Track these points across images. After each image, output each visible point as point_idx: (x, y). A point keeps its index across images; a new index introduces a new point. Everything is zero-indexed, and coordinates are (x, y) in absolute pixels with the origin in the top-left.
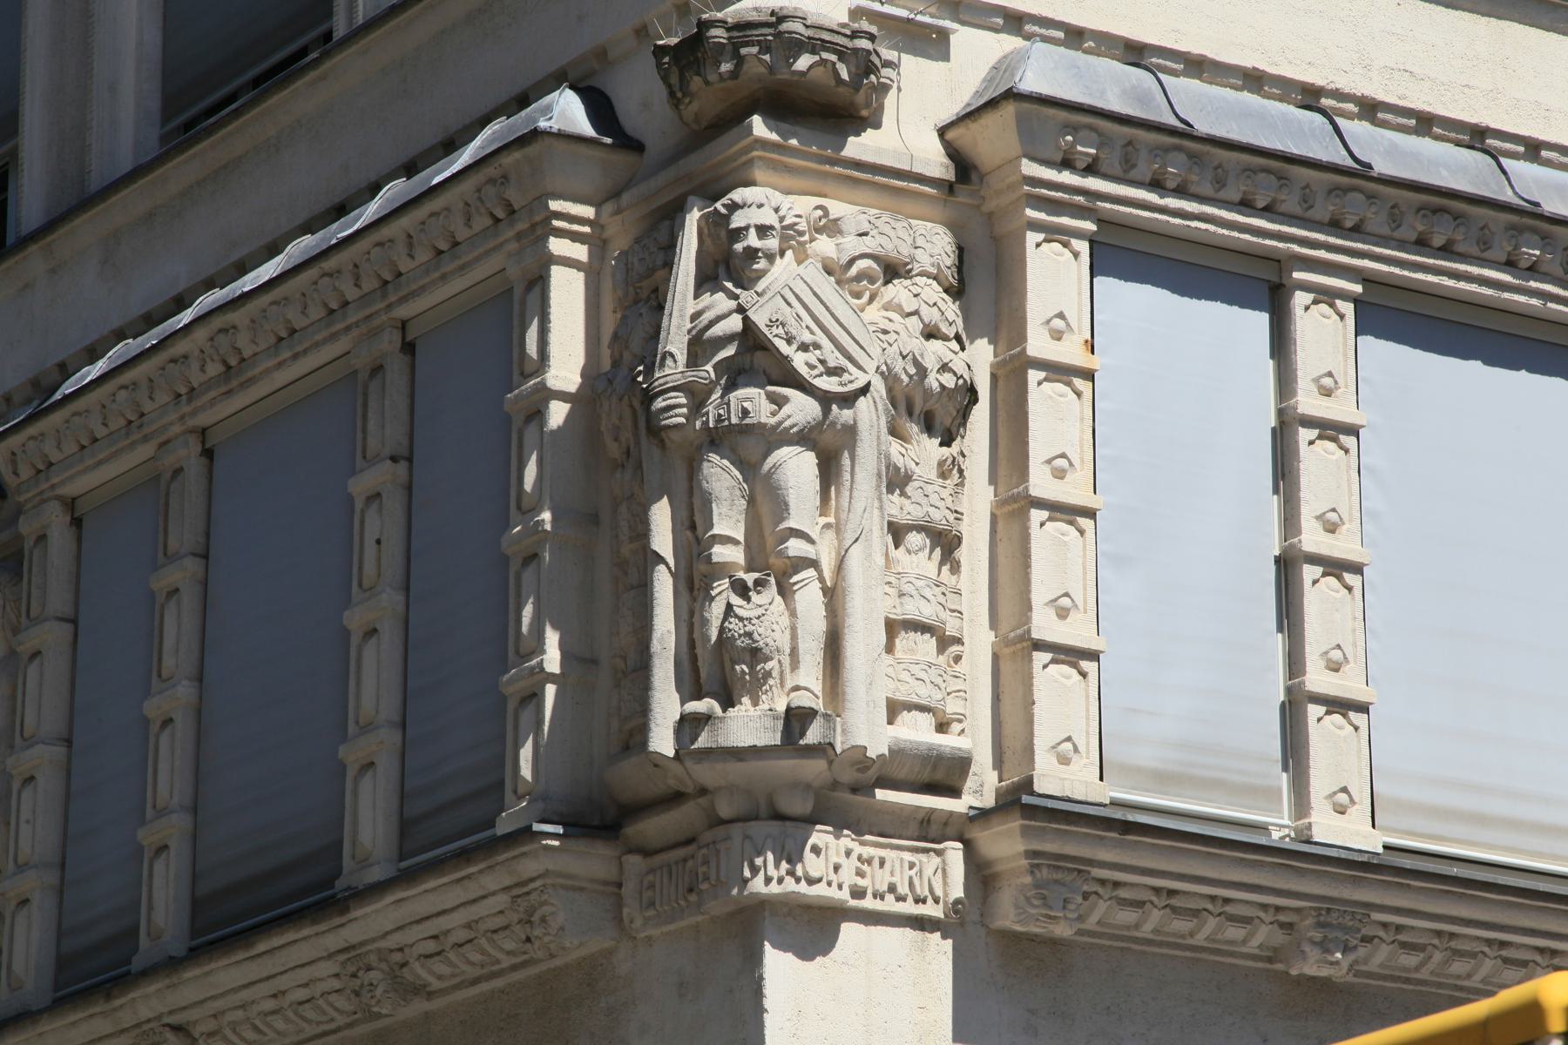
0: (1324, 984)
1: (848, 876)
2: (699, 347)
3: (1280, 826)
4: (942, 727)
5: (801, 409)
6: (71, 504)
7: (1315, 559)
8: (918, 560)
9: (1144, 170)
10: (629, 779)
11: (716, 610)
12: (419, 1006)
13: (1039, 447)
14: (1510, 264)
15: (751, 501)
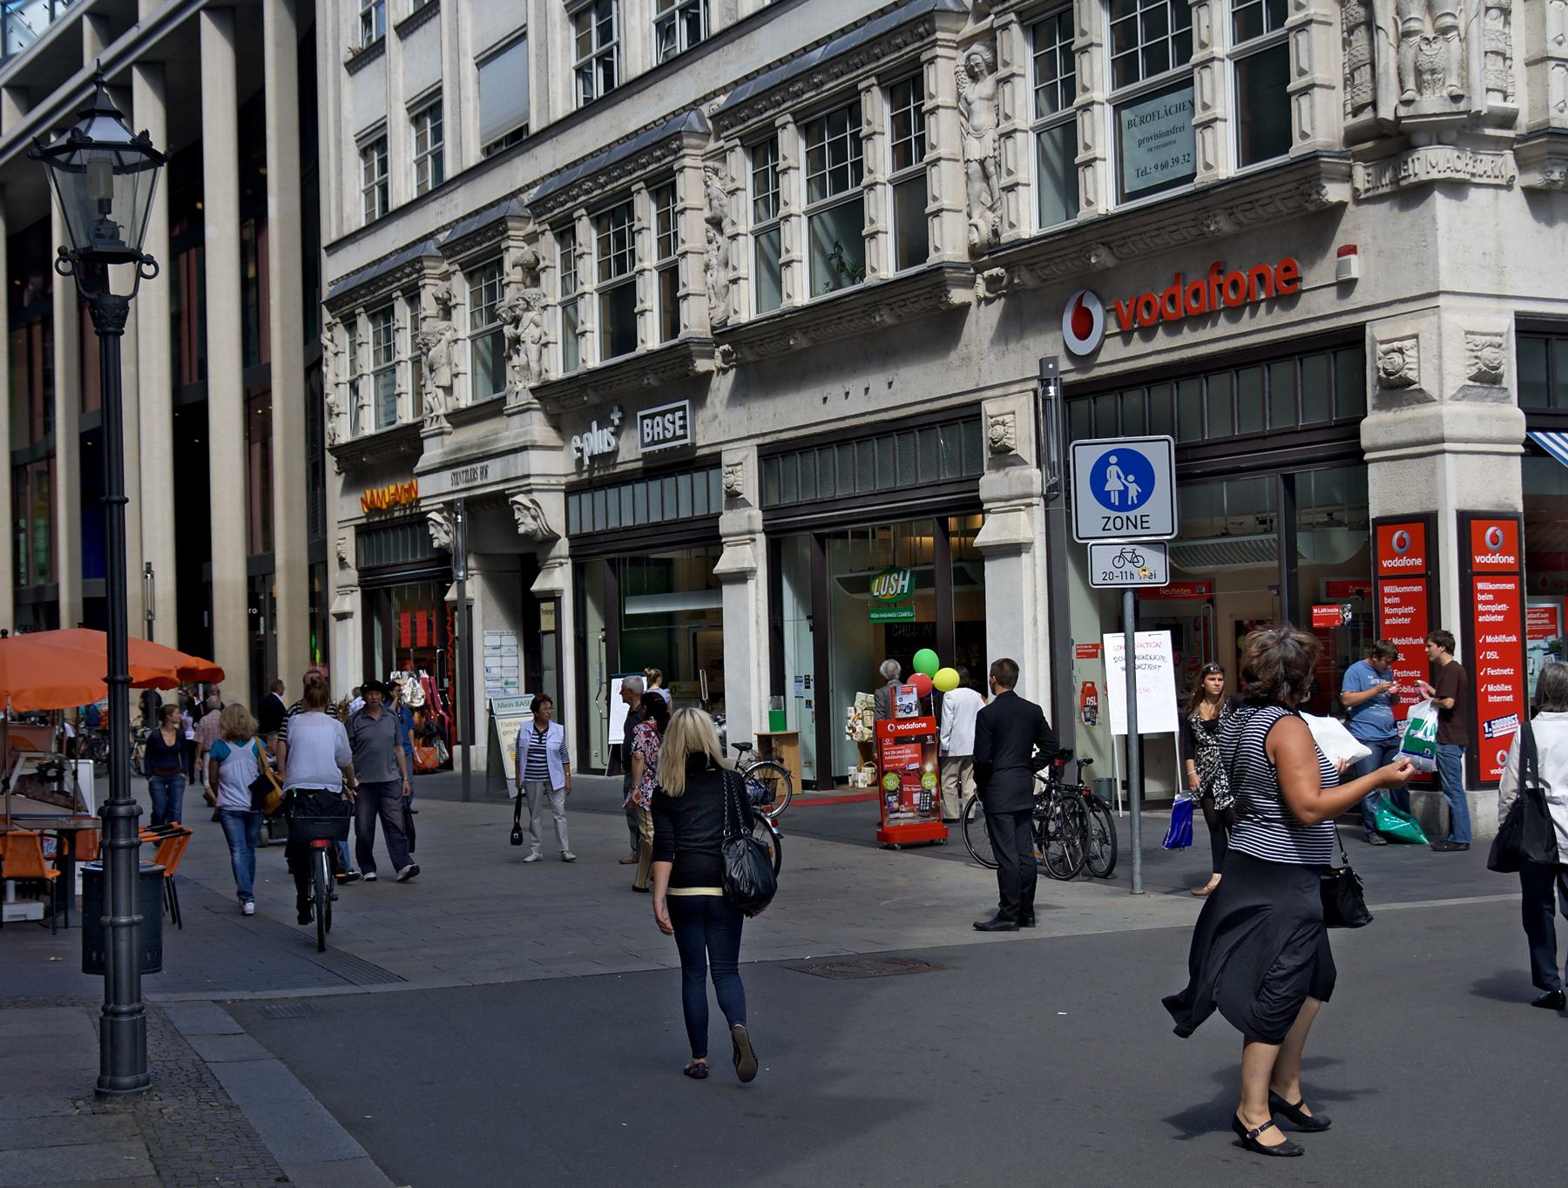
4: (1505, 99)
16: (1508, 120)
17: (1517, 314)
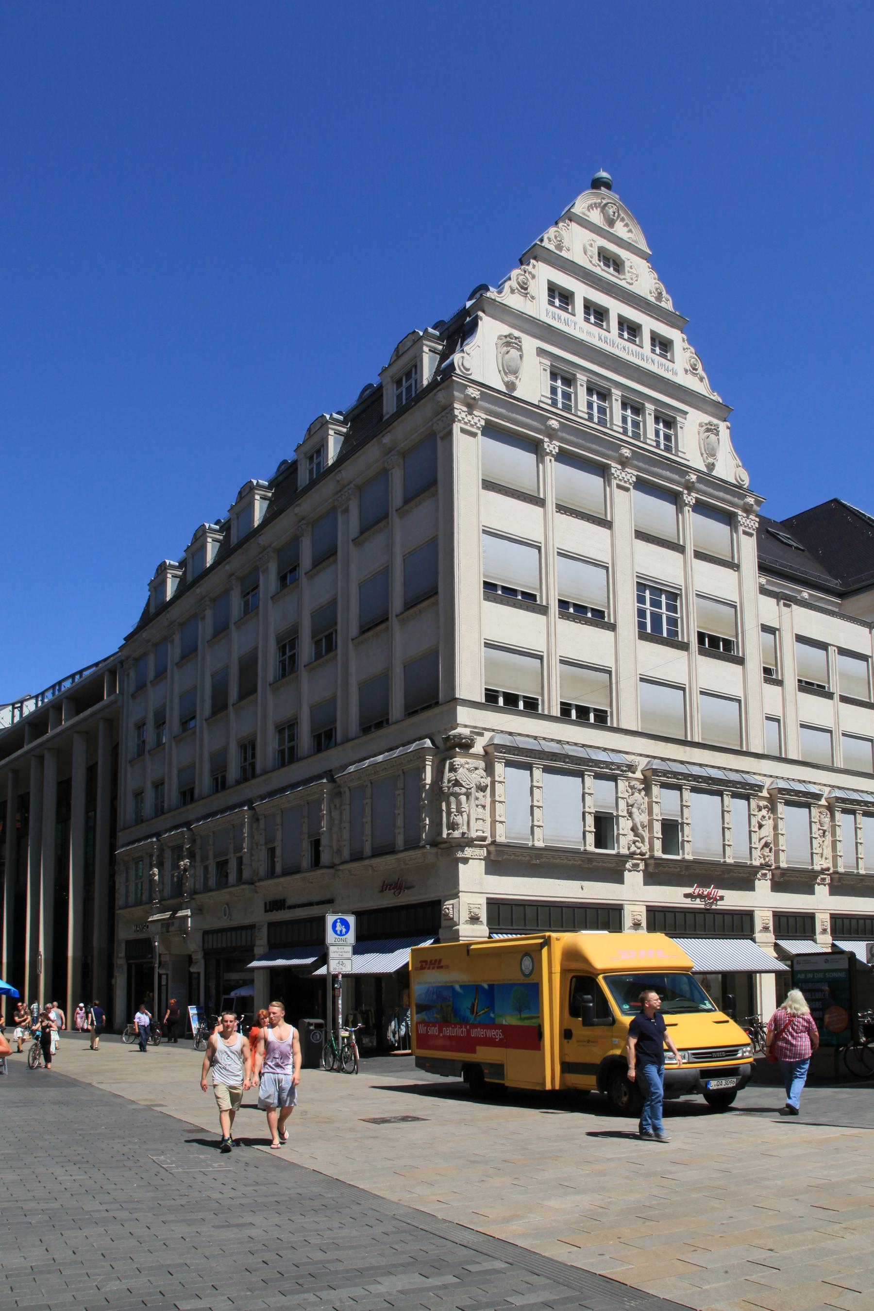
0: (536, 864)
1: (471, 854)
2: (449, 781)
3: (530, 844)
4: (483, 832)
5: (464, 790)
6: (349, 787)
7: (536, 806)
8: (480, 810)
9: (512, 753)
10: (438, 839)
11: (452, 818)
12: (408, 866)
13: (497, 794)
14: (564, 762)
15: (457, 803)
16: (484, 839)
17: (488, 899)
